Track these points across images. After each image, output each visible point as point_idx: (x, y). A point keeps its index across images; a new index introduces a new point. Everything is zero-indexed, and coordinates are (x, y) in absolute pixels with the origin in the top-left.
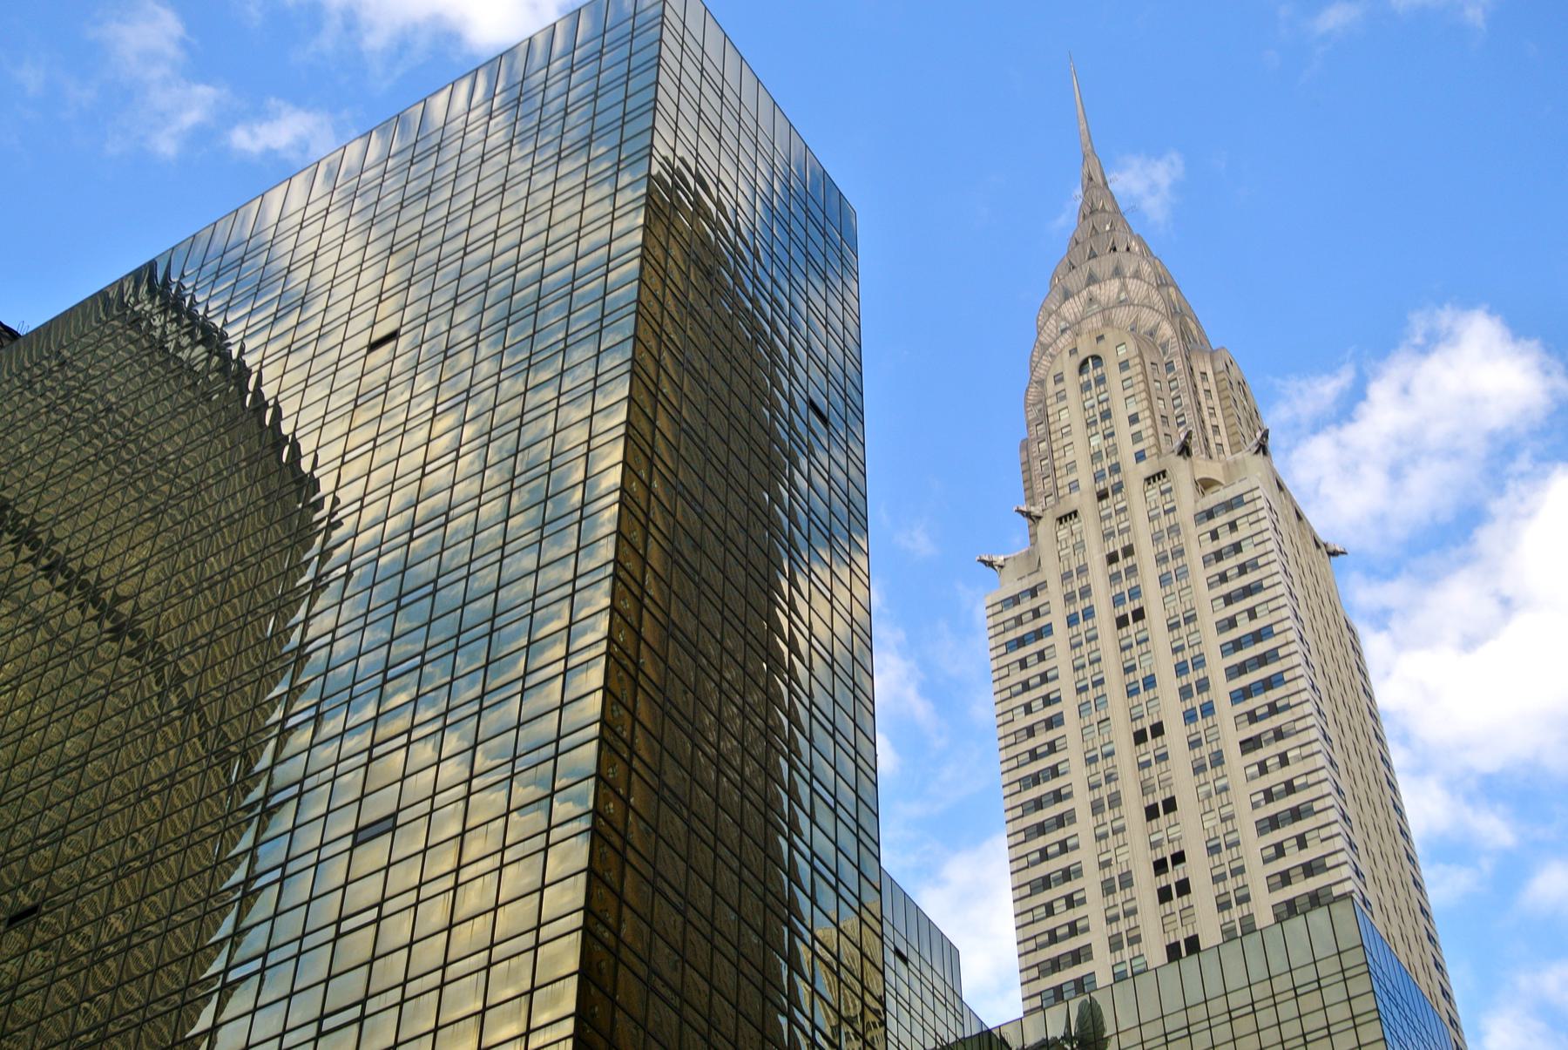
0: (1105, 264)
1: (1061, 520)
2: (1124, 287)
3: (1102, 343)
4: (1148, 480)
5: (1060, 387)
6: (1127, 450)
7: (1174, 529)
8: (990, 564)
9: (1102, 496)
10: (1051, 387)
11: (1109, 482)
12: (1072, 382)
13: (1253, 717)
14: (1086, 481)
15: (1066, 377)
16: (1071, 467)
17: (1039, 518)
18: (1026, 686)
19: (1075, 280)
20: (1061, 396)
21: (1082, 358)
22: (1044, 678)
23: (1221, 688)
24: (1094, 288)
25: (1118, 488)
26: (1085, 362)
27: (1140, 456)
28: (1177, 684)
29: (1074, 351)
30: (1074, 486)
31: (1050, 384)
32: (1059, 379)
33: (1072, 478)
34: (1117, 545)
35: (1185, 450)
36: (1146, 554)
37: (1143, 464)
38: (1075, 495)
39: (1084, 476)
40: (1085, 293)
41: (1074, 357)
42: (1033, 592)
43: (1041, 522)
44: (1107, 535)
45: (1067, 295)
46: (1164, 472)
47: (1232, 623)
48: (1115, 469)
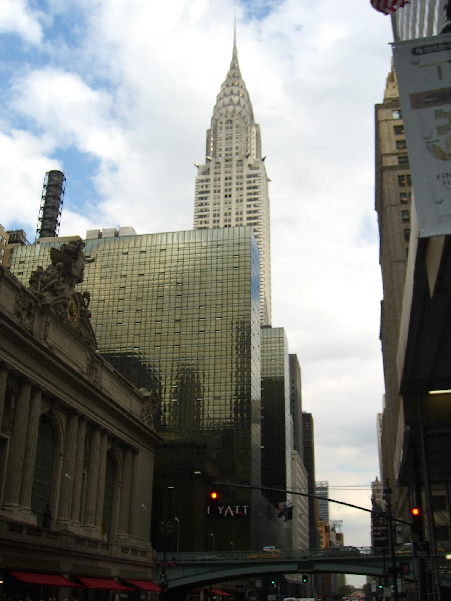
0: (235, 89)
1: (216, 163)
5: (221, 126)
6: (234, 151)
7: (242, 177)
8: (198, 166)
9: (227, 161)
10: (219, 125)
11: (229, 157)
12: (224, 126)
14: (223, 155)
16: (221, 150)
20: (221, 128)
22: (206, 204)
25: (231, 160)
27: (237, 154)
28: (236, 217)
29: (226, 117)
30: (220, 155)
32: (221, 123)
33: (220, 153)
34: (228, 175)
35: (247, 157)
36: (234, 181)
39: (223, 153)
42: (207, 180)
44: (226, 172)
45: (225, 95)
47: (249, 206)
48: (231, 155)
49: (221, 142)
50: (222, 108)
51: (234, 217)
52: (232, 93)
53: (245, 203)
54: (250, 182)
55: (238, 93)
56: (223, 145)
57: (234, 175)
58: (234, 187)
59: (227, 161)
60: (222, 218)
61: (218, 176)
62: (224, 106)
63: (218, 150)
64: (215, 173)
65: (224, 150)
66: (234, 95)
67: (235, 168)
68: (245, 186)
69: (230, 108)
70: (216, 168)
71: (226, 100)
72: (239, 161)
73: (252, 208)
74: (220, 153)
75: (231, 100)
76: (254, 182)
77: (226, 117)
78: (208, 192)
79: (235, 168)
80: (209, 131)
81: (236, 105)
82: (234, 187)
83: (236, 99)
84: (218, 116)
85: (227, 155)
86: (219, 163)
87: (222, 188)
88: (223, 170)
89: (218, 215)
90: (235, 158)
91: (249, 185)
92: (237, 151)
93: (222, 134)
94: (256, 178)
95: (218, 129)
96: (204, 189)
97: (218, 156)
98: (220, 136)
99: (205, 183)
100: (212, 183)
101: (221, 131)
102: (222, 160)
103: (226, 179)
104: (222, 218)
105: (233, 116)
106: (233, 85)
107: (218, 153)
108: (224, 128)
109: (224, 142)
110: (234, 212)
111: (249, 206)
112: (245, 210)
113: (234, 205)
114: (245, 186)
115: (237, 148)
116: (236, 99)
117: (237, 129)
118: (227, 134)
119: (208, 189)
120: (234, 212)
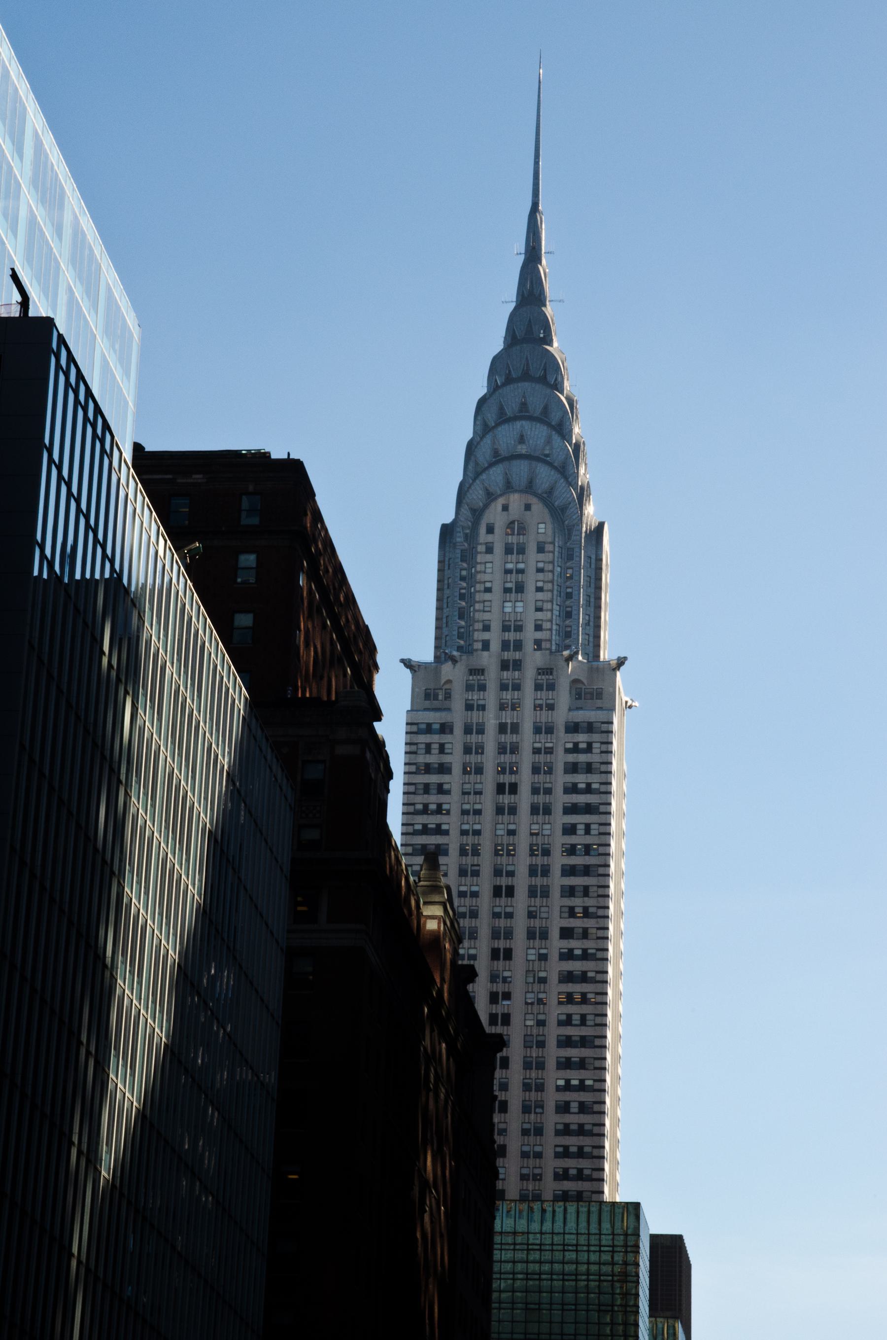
0: (535, 395)
1: (473, 671)
2: (549, 441)
3: (528, 513)
4: (538, 669)
5: (490, 538)
6: (529, 635)
10: (483, 536)
12: (498, 540)
13: (572, 913)
14: (495, 646)
15: (496, 530)
16: (487, 628)
17: (456, 662)
18: (425, 810)
19: (512, 397)
20: (489, 550)
21: (511, 518)
22: (439, 810)
23: (557, 881)
24: (526, 424)
26: (513, 522)
27: (538, 643)
29: (505, 508)
30: (486, 646)
31: (483, 530)
32: (490, 530)
33: (486, 636)
34: (508, 717)
36: (527, 738)
37: (538, 653)
38: (485, 653)
39: (495, 637)
40: (518, 424)
41: (505, 513)
42: (445, 728)
43: (458, 665)
45: (503, 419)
46: (552, 669)
48: (518, 645)
49: (487, 596)
50: (491, 465)
51: (522, 862)
52: (523, 413)
53: (560, 819)
54: (575, 749)
55: (546, 410)
56: (494, 608)
57: (528, 719)
58: (526, 760)
59: (505, 665)
60: (486, 862)
61: (475, 717)
62: (498, 458)
64: (469, 707)
65: (496, 626)
66: (531, 418)
67: (529, 696)
68: (561, 759)
69: (520, 470)
70: (469, 688)
71: (506, 437)
72: (541, 671)
73: (579, 839)
74: (486, 636)
75: (522, 440)
76: (589, 749)
77: (505, 508)
78: (444, 769)
79: (529, 696)
80: (446, 532)
81: (537, 459)
82: (526, 760)
83: (537, 434)
84: (477, 495)
85: (505, 646)
86: (481, 671)
87: (490, 759)
88: (491, 697)
89: (476, 852)
90: (533, 659)
91: (571, 758)
92: (539, 635)
93: (491, 569)
94: (596, 737)
95: (481, 548)
96: (433, 759)
98: (487, 577)
99: (435, 738)
100: (456, 740)
101: (489, 557)
102: (489, 660)
103: (502, 728)
104: (486, 862)
105: (528, 507)
106: (526, 376)
108: (499, 549)
109: (496, 596)
110: (523, 843)
111: (570, 830)
112: (559, 841)
113: (524, 820)
114: (561, 759)
115: (538, 628)
117: (541, 556)
118: (508, 572)
119: (446, 759)
120: (523, 843)
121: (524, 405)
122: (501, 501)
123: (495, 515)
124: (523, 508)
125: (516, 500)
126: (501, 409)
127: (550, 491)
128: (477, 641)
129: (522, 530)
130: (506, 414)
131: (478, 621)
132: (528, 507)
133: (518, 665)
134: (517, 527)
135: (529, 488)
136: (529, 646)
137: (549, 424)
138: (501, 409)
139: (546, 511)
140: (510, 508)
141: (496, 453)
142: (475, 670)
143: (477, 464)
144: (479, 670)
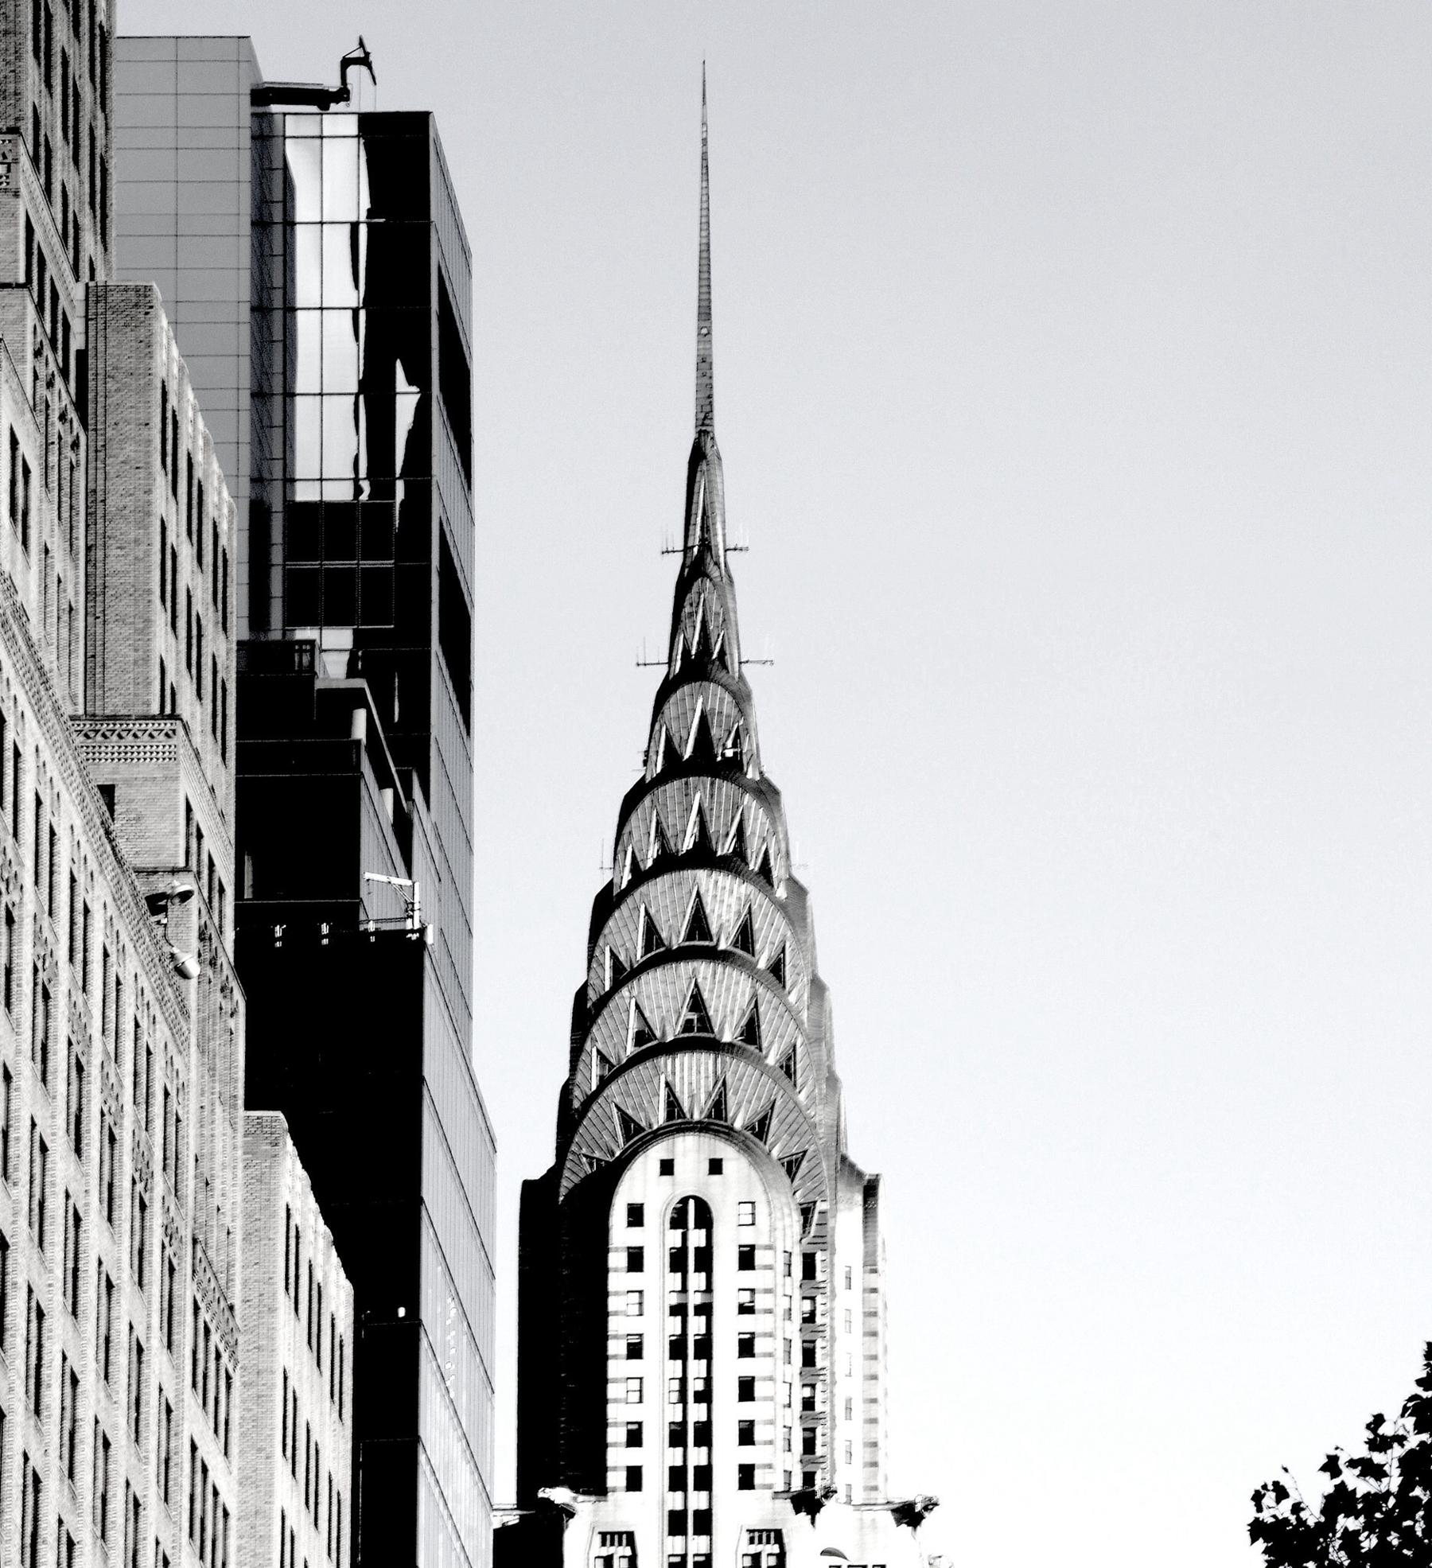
1: (608, 1538)
6: (727, 1456)
10: (621, 1235)
14: (655, 1479)
16: (635, 1438)
19: (667, 903)
20: (636, 1260)
26: (684, 1201)
27: (747, 1477)
29: (667, 1167)
30: (634, 1478)
31: (618, 1216)
32: (636, 1215)
33: (633, 1457)
39: (656, 1457)
40: (685, 968)
48: (704, 1480)
52: (699, 944)
55: (746, 937)
59: (677, 1523)
63: (616, 1435)
65: (656, 1435)
66: (713, 955)
69: (692, 1076)
71: (661, 998)
72: (757, 1535)
74: (633, 1457)
75: (697, 1003)
77: (667, 1167)
97: (616, 1479)
105: (716, 1167)
107: (619, 1457)
116: (729, 996)
121: (699, 923)
122: (656, 1153)
123: (641, 1183)
124: (706, 1166)
125: (690, 1151)
126: (651, 931)
127: (760, 1128)
128: (615, 1469)
129: (705, 1218)
130: (660, 943)
131: (616, 1424)
132: (716, 1167)
133: (704, 1522)
134: (694, 1213)
135: (715, 1123)
136: (725, 1477)
137: (750, 969)
138: (651, 931)
139: (754, 1176)
140: (677, 1168)
141: (641, 1037)
142: (612, 1534)
143: (603, 1059)
144: (620, 1534)
